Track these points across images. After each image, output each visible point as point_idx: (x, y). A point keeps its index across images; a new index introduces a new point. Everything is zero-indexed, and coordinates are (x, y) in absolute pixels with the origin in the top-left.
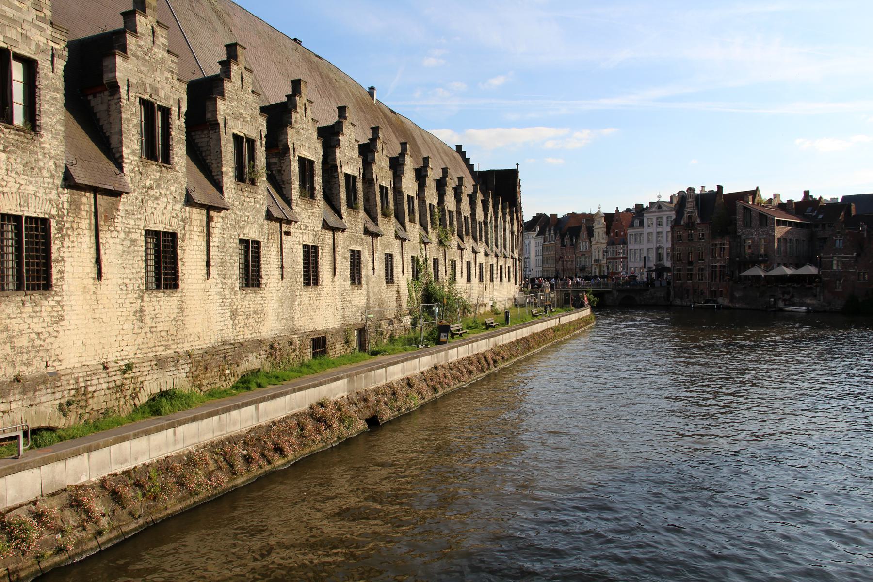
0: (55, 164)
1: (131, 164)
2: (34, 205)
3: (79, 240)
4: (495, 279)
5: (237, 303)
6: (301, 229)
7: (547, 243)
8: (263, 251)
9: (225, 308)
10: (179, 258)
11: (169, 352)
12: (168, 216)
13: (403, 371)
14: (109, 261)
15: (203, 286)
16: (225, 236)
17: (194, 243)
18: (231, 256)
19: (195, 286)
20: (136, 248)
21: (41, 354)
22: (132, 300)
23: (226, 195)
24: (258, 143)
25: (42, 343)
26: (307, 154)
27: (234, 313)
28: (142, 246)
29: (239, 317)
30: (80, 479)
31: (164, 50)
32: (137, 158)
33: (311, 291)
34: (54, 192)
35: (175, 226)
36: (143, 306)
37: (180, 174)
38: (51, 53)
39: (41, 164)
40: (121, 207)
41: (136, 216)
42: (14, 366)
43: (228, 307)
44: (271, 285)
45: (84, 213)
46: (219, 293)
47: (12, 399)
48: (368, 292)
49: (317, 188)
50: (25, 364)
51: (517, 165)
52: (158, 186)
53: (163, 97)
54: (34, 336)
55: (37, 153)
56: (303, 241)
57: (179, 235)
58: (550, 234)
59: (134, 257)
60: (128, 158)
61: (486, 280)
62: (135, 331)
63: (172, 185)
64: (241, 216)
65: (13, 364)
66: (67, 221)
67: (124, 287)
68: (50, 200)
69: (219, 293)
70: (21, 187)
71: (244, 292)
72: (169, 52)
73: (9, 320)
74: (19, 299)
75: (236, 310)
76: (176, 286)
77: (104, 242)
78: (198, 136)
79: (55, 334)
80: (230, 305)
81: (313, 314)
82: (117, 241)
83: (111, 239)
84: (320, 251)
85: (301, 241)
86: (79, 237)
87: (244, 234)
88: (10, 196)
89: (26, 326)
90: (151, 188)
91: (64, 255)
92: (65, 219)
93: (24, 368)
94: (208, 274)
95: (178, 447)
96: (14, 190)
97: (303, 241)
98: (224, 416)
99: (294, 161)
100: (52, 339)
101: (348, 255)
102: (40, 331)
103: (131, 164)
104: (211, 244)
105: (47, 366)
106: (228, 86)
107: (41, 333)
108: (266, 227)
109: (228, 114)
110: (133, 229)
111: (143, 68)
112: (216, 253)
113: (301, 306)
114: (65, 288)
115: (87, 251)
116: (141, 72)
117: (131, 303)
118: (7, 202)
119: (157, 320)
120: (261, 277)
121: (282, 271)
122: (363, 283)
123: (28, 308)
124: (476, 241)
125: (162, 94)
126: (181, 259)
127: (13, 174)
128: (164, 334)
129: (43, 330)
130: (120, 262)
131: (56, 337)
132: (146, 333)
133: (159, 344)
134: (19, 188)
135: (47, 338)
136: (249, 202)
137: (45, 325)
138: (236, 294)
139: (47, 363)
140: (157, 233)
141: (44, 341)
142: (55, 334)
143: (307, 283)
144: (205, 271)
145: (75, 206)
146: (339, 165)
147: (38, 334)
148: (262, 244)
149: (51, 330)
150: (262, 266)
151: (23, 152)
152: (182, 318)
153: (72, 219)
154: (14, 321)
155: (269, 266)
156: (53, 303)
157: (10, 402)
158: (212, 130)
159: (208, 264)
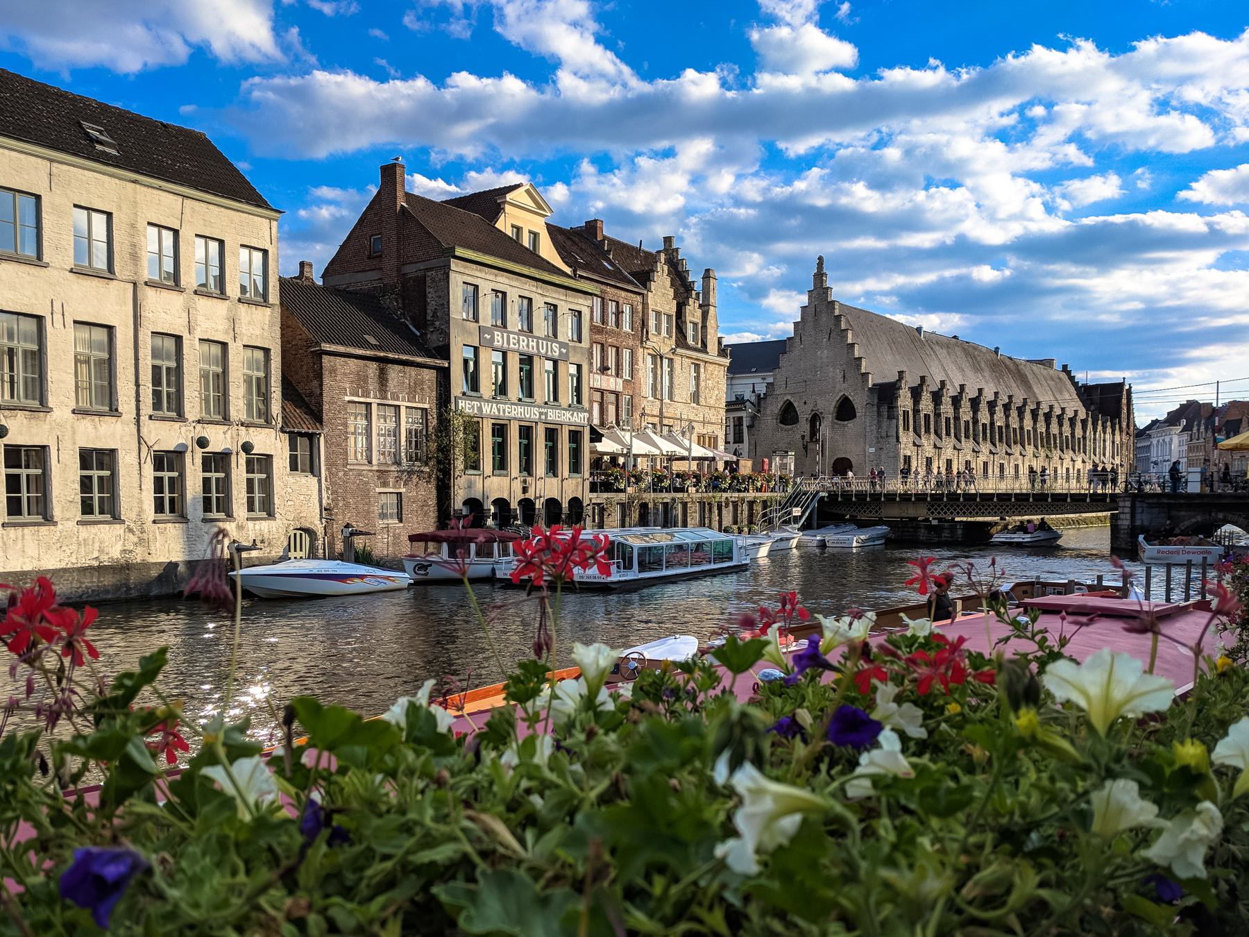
7: (1195, 441)
58: (1198, 430)
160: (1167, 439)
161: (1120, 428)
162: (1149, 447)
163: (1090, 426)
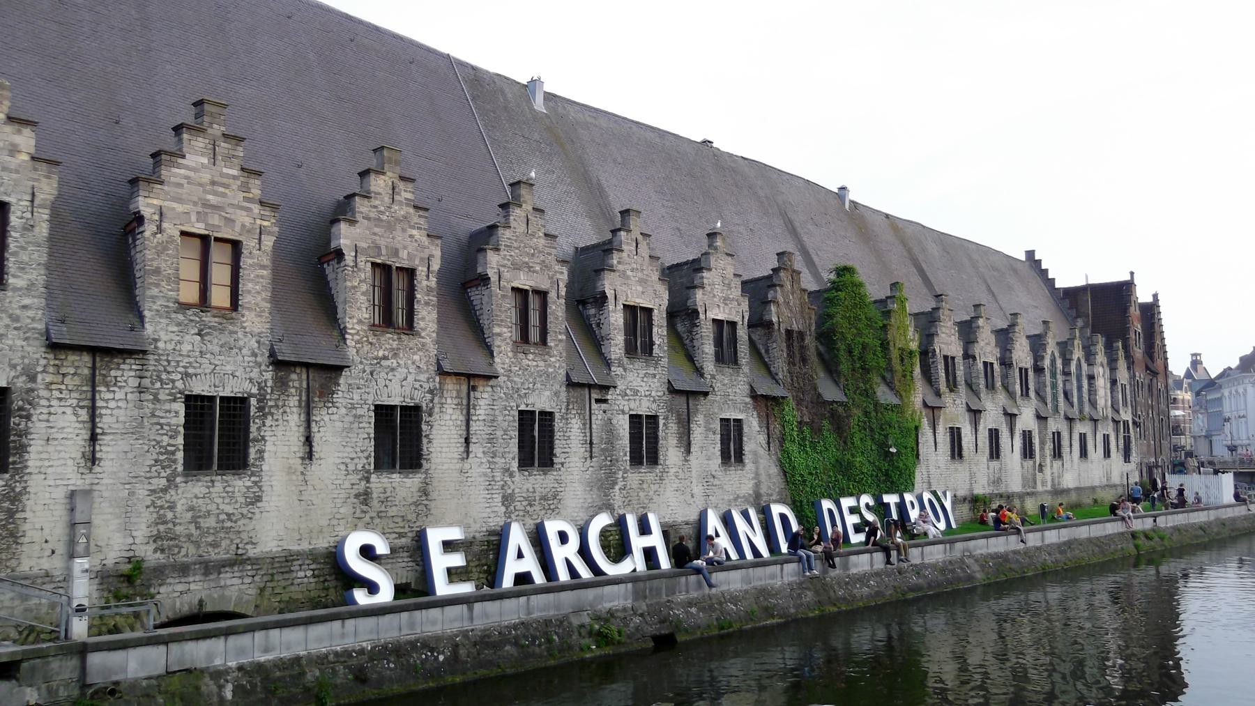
0: (258, 342)
1: (357, 333)
2: (230, 385)
3: (285, 418)
4: (1064, 455)
5: (512, 487)
6: (626, 395)
8: (558, 424)
9: (494, 492)
10: (424, 434)
11: (403, 540)
12: (408, 390)
13: (747, 580)
14: (324, 439)
15: (458, 466)
16: (495, 407)
17: (448, 417)
18: (505, 431)
19: (446, 466)
20: (361, 425)
21: (232, 536)
22: (353, 482)
23: (497, 360)
24: (552, 295)
25: (233, 525)
26: (638, 301)
27: (507, 500)
28: (370, 423)
29: (519, 503)
30: (213, 662)
31: (407, 205)
32: (365, 328)
33: (646, 474)
34: (256, 370)
35: (421, 398)
36: (368, 488)
37: (428, 340)
38: (258, 230)
39: (241, 343)
40: (342, 381)
41: (363, 391)
42: (198, 547)
43: (498, 491)
44: (571, 465)
45: (293, 391)
46: (485, 475)
47: (191, 579)
48: (757, 474)
49: (657, 342)
50: (211, 545)
51: (1132, 274)
52: (396, 355)
53: (405, 257)
54: (223, 517)
55: (236, 333)
56: (630, 410)
57: (424, 408)
59: (358, 434)
60: (352, 329)
61: (1043, 456)
62: (357, 515)
63: (414, 354)
64: (523, 383)
65: (197, 544)
66: (270, 400)
67: (343, 467)
68: (251, 380)
69: (485, 475)
70: (217, 368)
71: (527, 473)
72: (416, 207)
73: (195, 500)
74: (208, 478)
75: (512, 495)
76: (419, 466)
77: (318, 419)
78: (473, 293)
79: (250, 515)
80: (502, 489)
81: (646, 501)
82: (334, 417)
83: (328, 416)
84: (661, 422)
85: (626, 409)
86: (285, 415)
87: (527, 405)
88: (203, 377)
89: (214, 506)
90: (385, 358)
91: (266, 434)
92: (268, 397)
93: (210, 549)
94: (468, 452)
95: (346, 641)
96: (208, 371)
97: (630, 410)
98: (417, 614)
99: (615, 311)
100: (247, 521)
101: (717, 426)
102: (231, 512)
103: (357, 333)
104: (474, 418)
105: (238, 548)
106: (504, 235)
107: (233, 514)
108: (563, 395)
109: (504, 266)
110: (358, 404)
111: (377, 230)
112: (481, 428)
113: (625, 492)
114: (264, 468)
115: (296, 428)
116: (375, 234)
117: (352, 484)
118: (200, 384)
119: (389, 503)
120: (555, 455)
121: (591, 447)
122: (747, 461)
123: (219, 486)
124: (1011, 395)
125: (404, 254)
126: (427, 436)
127: (208, 356)
128: (399, 520)
129: (235, 511)
130: (339, 440)
131: (251, 518)
132: (372, 518)
133: (391, 531)
134: (214, 369)
135: (240, 519)
136: (537, 366)
137: (237, 506)
138: (511, 475)
139: (237, 545)
140: (393, 408)
141: (235, 522)
142: (250, 515)
143: (636, 460)
144: (462, 449)
145: (281, 384)
146: (701, 310)
147: (228, 515)
148: (557, 416)
149: (245, 511)
150: (557, 442)
151: (220, 333)
152: (425, 502)
153: (277, 397)
154: (200, 501)
155: (568, 442)
156: (249, 484)
157: (189, 583)
158: (484, 286)
159: (467, 441)
160: (1241, 390)
161: (1129, 357)
162: (1220, 400)
163: (1078, 353)
